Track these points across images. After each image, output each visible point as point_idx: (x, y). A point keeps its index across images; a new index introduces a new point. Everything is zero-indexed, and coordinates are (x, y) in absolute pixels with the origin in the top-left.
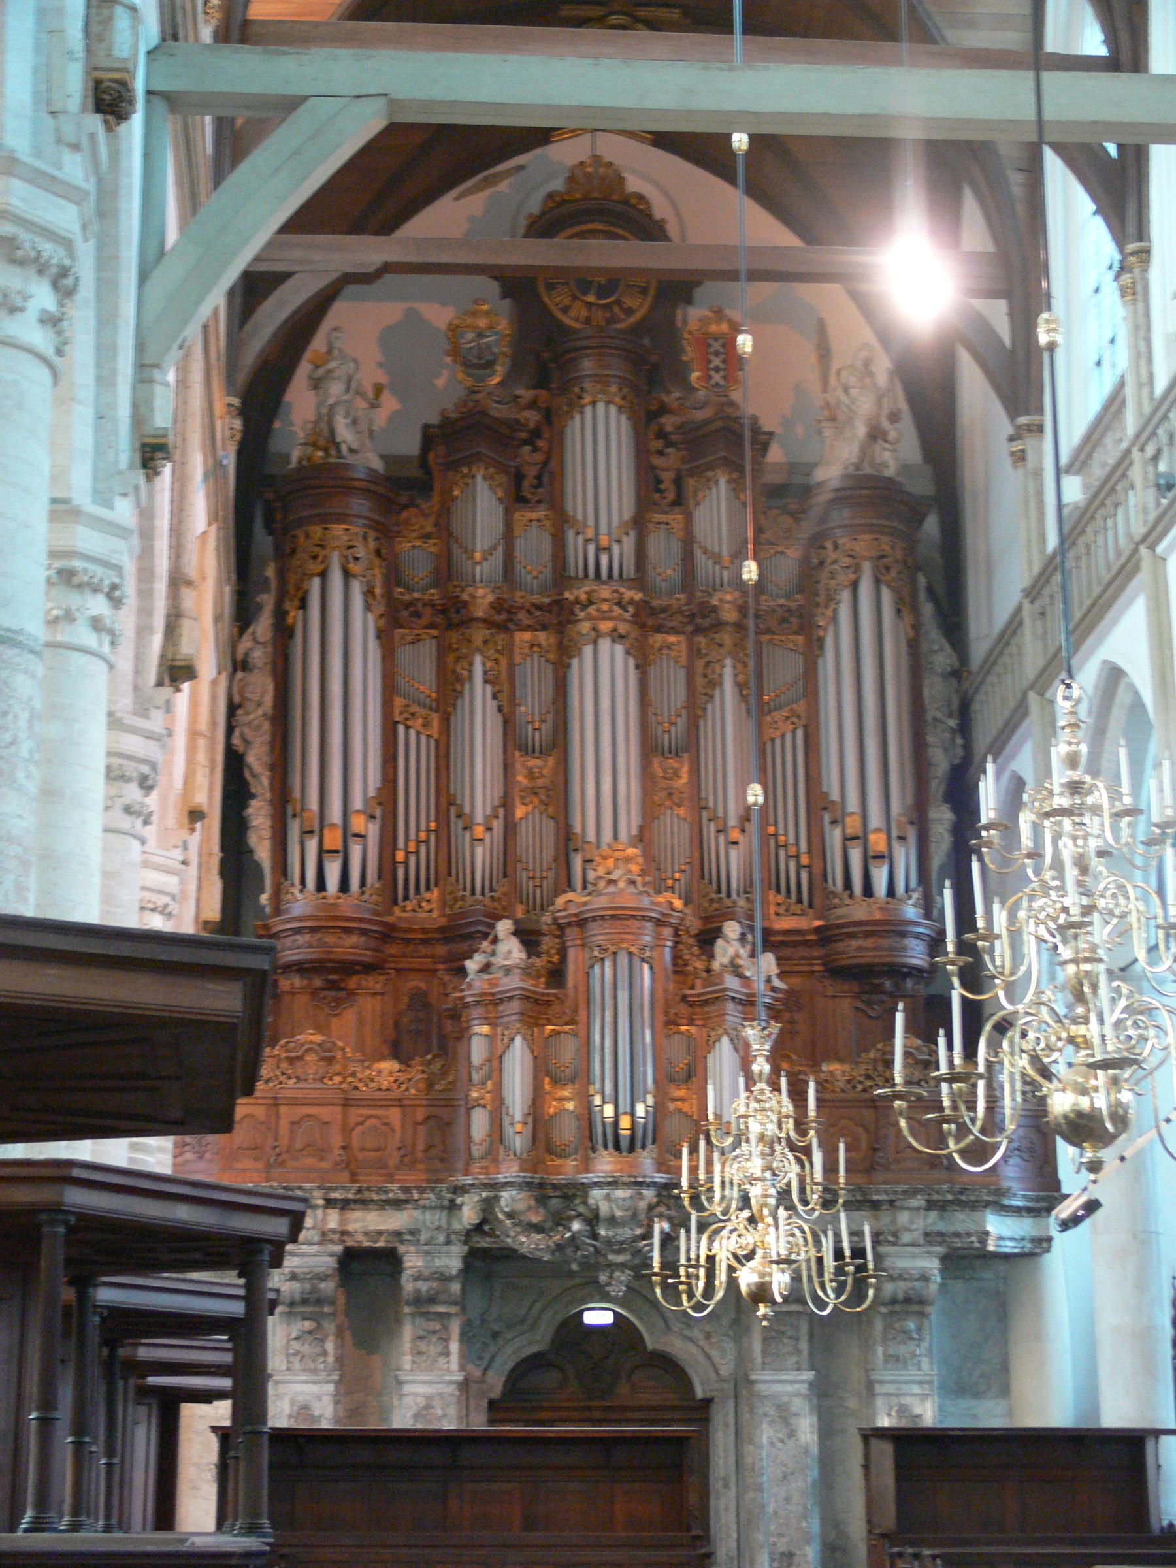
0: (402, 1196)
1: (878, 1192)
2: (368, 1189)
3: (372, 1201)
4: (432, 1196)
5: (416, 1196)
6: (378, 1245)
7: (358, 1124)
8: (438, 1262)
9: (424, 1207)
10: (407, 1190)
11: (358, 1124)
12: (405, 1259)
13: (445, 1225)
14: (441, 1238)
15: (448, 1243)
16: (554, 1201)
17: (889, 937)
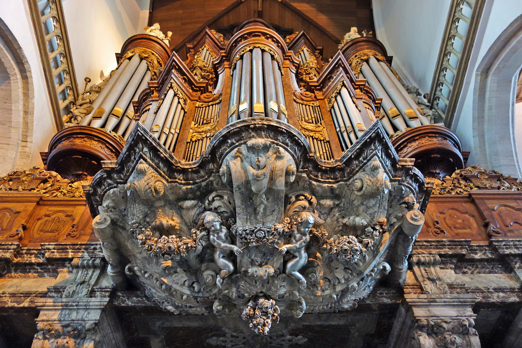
0: (57, 255)
1: (508, 247)
2: (29, 251)
3: (31, 264)
4: (86, 255)
5: (70, 255)
6: (21, 305)
7: (46, 216)
8: (74, 315)
9: (77, 267)
10: (63, 249)
11: (46, 216)
12: (41, 313)
13: (93, 282)
14: (85, 291)
15: (92, 293)
16: (188, 203)
17: (436, 137)
